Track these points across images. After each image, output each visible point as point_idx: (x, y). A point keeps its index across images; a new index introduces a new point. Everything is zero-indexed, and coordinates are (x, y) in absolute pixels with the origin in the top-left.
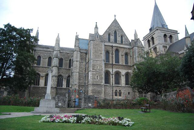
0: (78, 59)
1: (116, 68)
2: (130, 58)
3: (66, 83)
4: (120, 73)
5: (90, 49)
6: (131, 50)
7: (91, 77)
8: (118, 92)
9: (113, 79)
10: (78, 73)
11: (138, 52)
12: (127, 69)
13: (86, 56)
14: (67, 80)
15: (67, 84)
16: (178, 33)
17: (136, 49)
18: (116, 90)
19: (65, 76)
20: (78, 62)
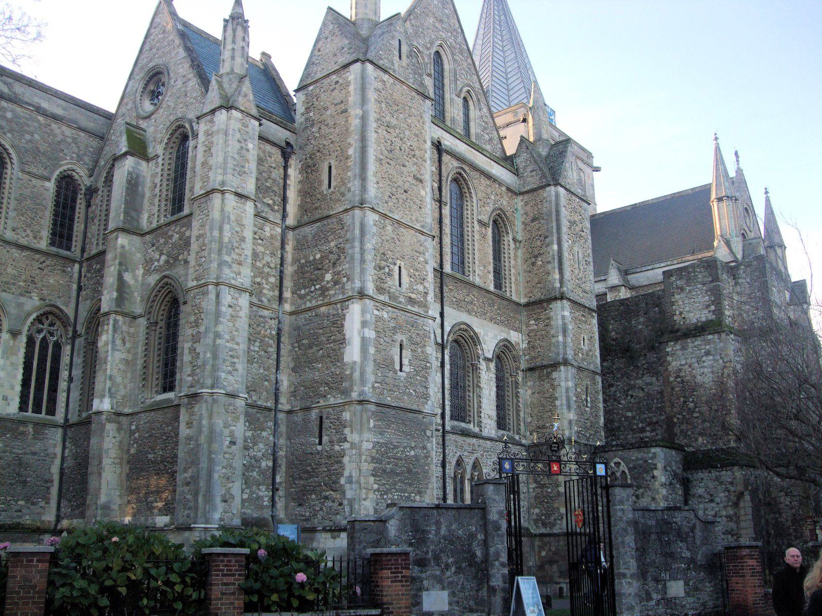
0: (250, 187)
1: (459, 305)
2: (512, 252)
3: (20, 377)
4: (475, 340)
5: (355, 122)
6: (519, 202)
7: (372, 350)
8: (468, 476)
9: (447, 381)
10: (244, 301)
11: (572, 223)
12: (501, 323)
13: (286, 176)
14: (30, 342)
15: (26, 383)
16: (595, 164)
17: (563, 201)
18: (459, 463)
19: (13, 310)
20: (249, 207)
